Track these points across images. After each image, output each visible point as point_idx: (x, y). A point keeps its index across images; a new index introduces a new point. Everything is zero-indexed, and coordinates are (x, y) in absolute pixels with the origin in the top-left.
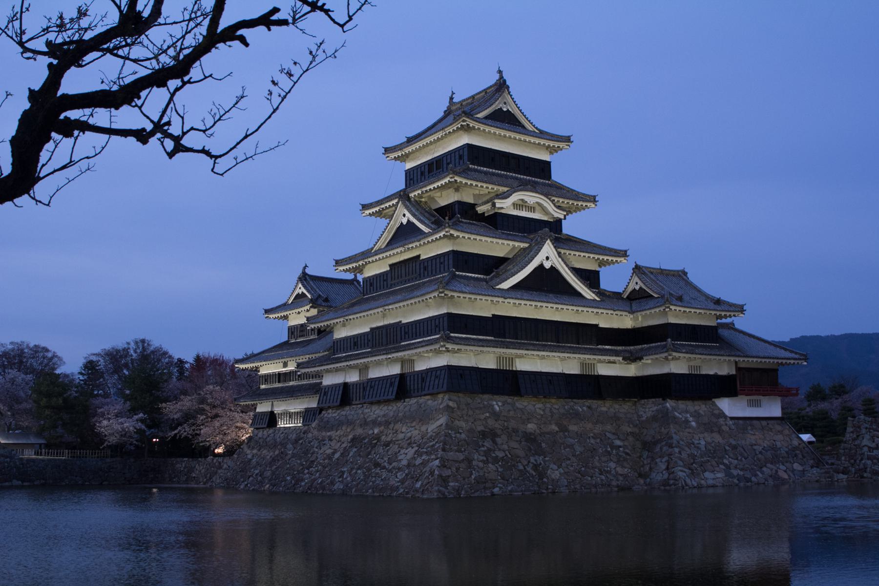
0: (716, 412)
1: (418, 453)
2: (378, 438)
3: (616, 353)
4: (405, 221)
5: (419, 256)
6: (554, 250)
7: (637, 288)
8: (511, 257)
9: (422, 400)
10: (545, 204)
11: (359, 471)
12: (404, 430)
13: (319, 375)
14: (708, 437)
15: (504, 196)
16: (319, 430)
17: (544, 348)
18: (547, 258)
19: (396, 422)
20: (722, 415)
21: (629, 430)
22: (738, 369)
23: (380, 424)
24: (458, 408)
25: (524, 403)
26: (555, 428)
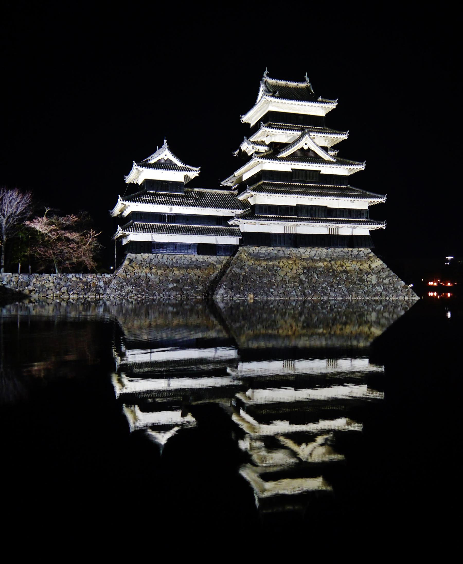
4: (306, 148)
5: (320, 171)
9: (345, 250)
16: (256, 260)
23: (320, 260)
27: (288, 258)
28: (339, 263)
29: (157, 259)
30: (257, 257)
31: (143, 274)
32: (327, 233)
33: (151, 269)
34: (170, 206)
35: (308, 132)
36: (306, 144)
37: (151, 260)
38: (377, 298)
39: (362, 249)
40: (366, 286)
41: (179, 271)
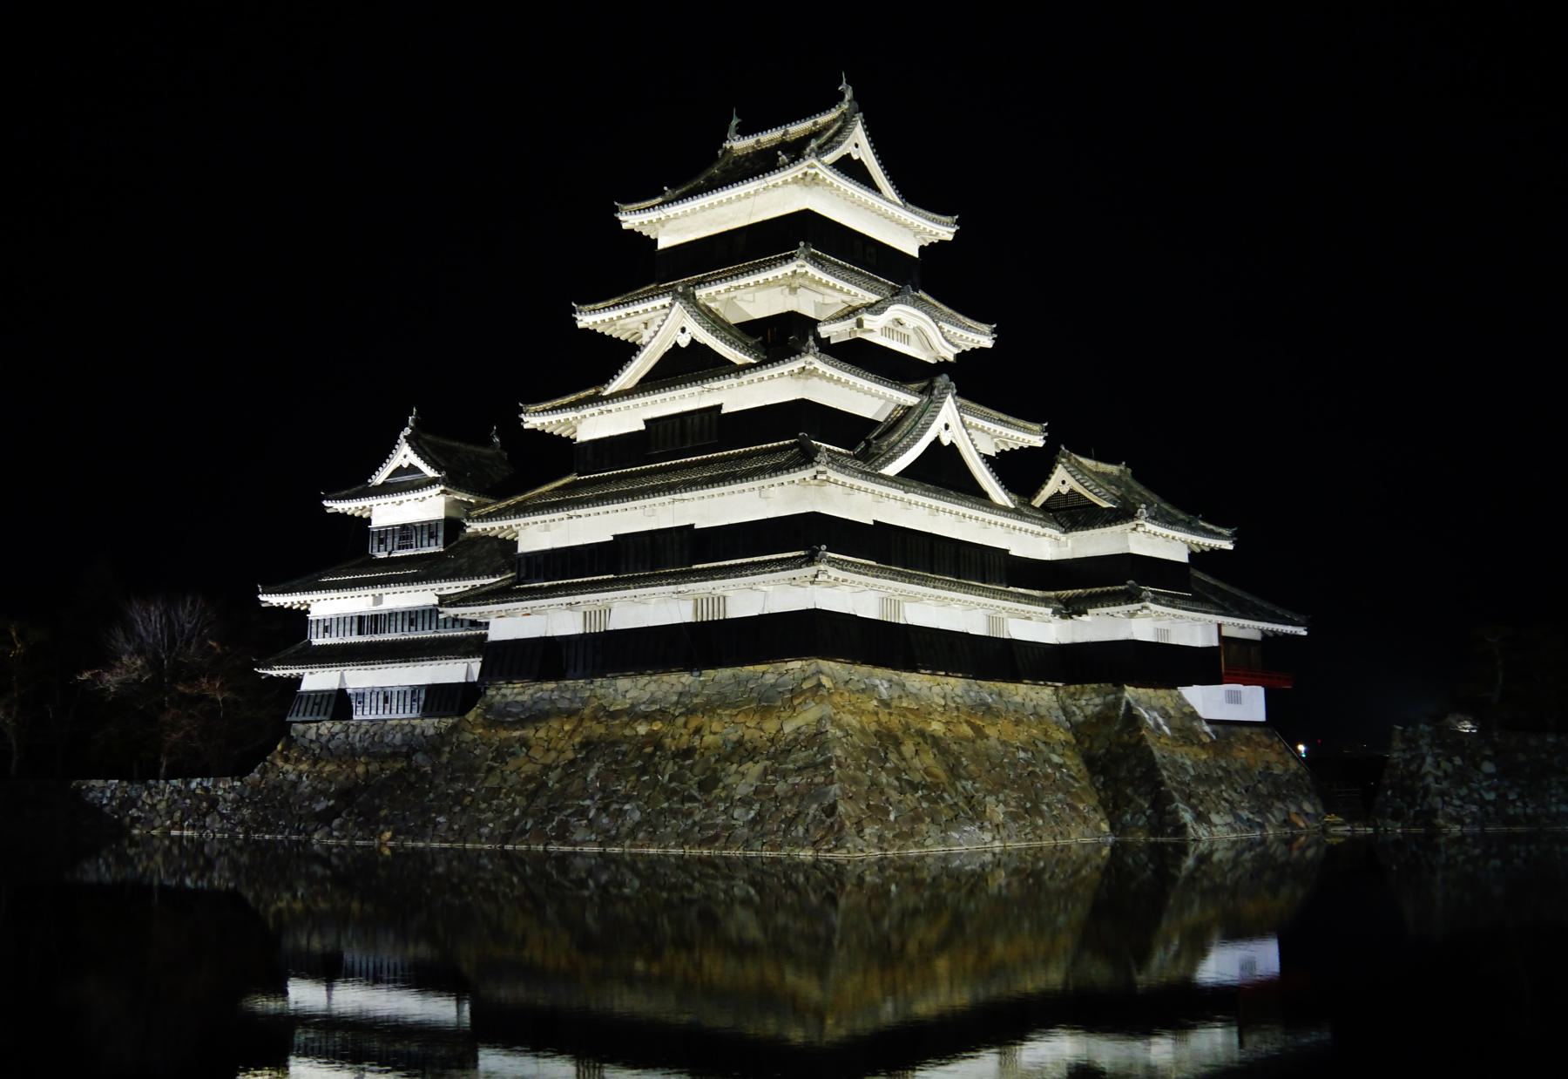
0: (1186, 710)
4: (684, 342)
5: (720, 407)
7: (1064, 490)
11: (627, 807)
12: (716, 726)
18: (947, 427)
19: (690, 712)
22: (1222, 638)
23: (648, 717)
27: (570, 713)
28: (693, 723)
29: (342, 736)
30: (501, 717)
31: (292, 777)
32: (688, 617)
33: (316, 760)
34: (378, 591)
35: (687, 287)
36: (683, 330)
37: (333, 736)
38: (706, 852)
39: (796, 665)
40: (708, 805)
41: (367, 764)
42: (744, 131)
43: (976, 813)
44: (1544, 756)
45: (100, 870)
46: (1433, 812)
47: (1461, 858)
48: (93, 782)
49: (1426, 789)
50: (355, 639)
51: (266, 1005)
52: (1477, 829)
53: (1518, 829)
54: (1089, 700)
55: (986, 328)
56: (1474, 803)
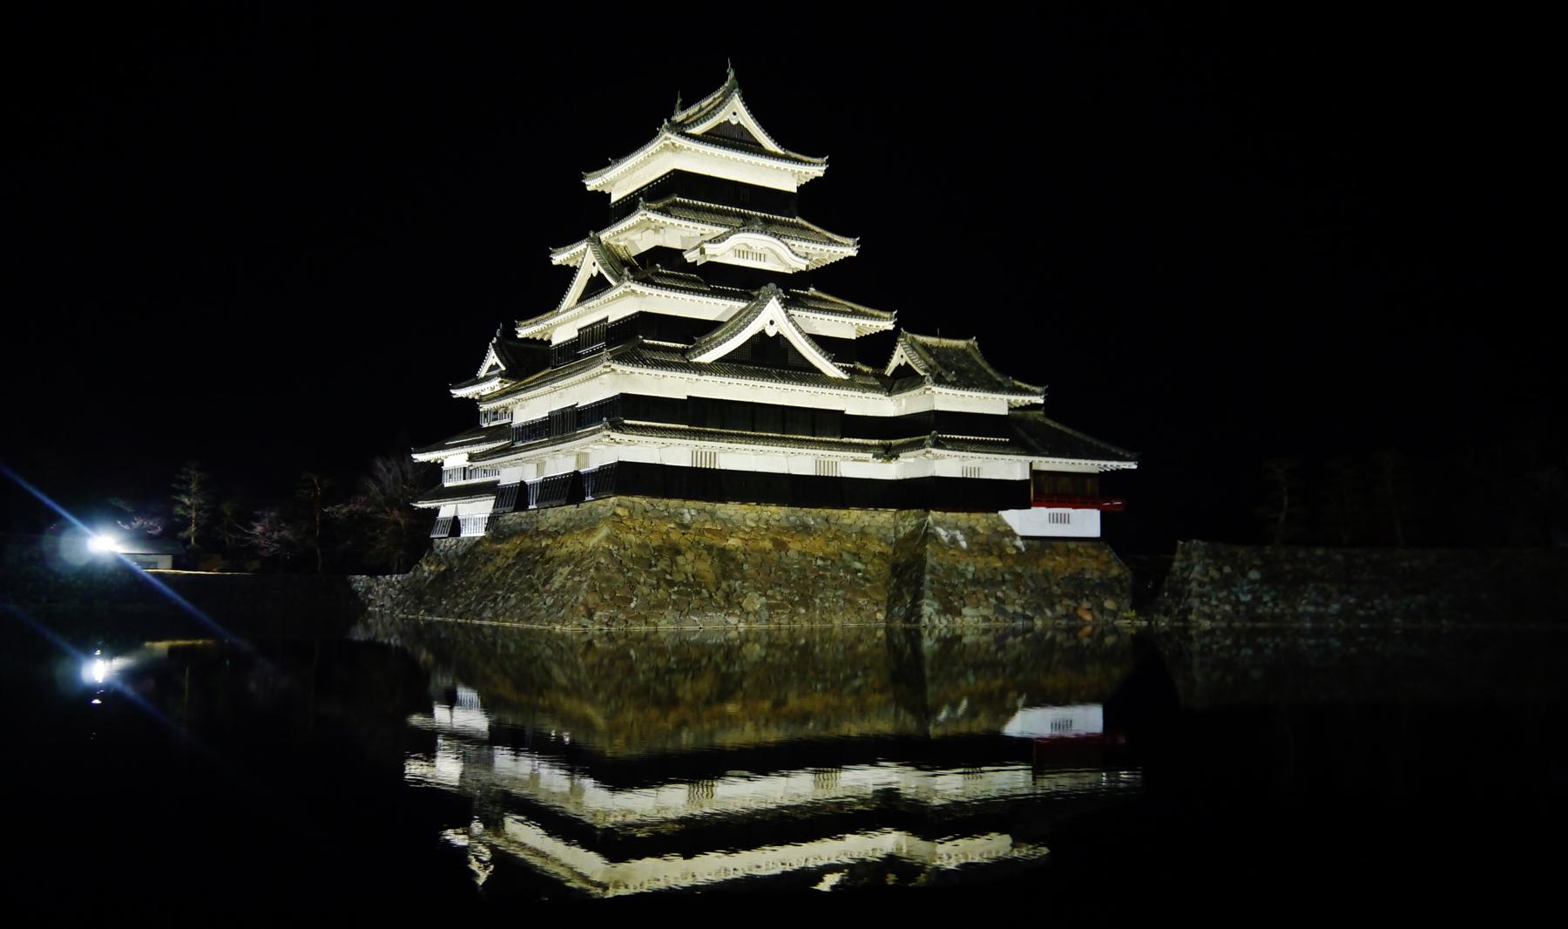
1: (572, 573)
2: (542, 552)
3: (864, 448)
6: (782, 312)
8: (725, 320)
10: (778, 250)
13: (496, 472)
14: (981, 561)
15: (717, 240)
17: (756, 439)
20: (1011, 533)
21: (878, 549)
22: (1034, 473)
24: (631, 516)
25: (731, 510)
26: (768, 544)
42: (683, 109)
43: (731, 602)
44: (1309, 566)
45: (358, 634)
46: (1189, 610)
47: (1215, 647)
48: (358, 577)
49: (1190, 591)
50: (462, 482)
51: (416, 720)
52: (1224, 624)
53: (1261, 625)
54: (908, 521)
55: (850, 241)
56: (1229, 603)
